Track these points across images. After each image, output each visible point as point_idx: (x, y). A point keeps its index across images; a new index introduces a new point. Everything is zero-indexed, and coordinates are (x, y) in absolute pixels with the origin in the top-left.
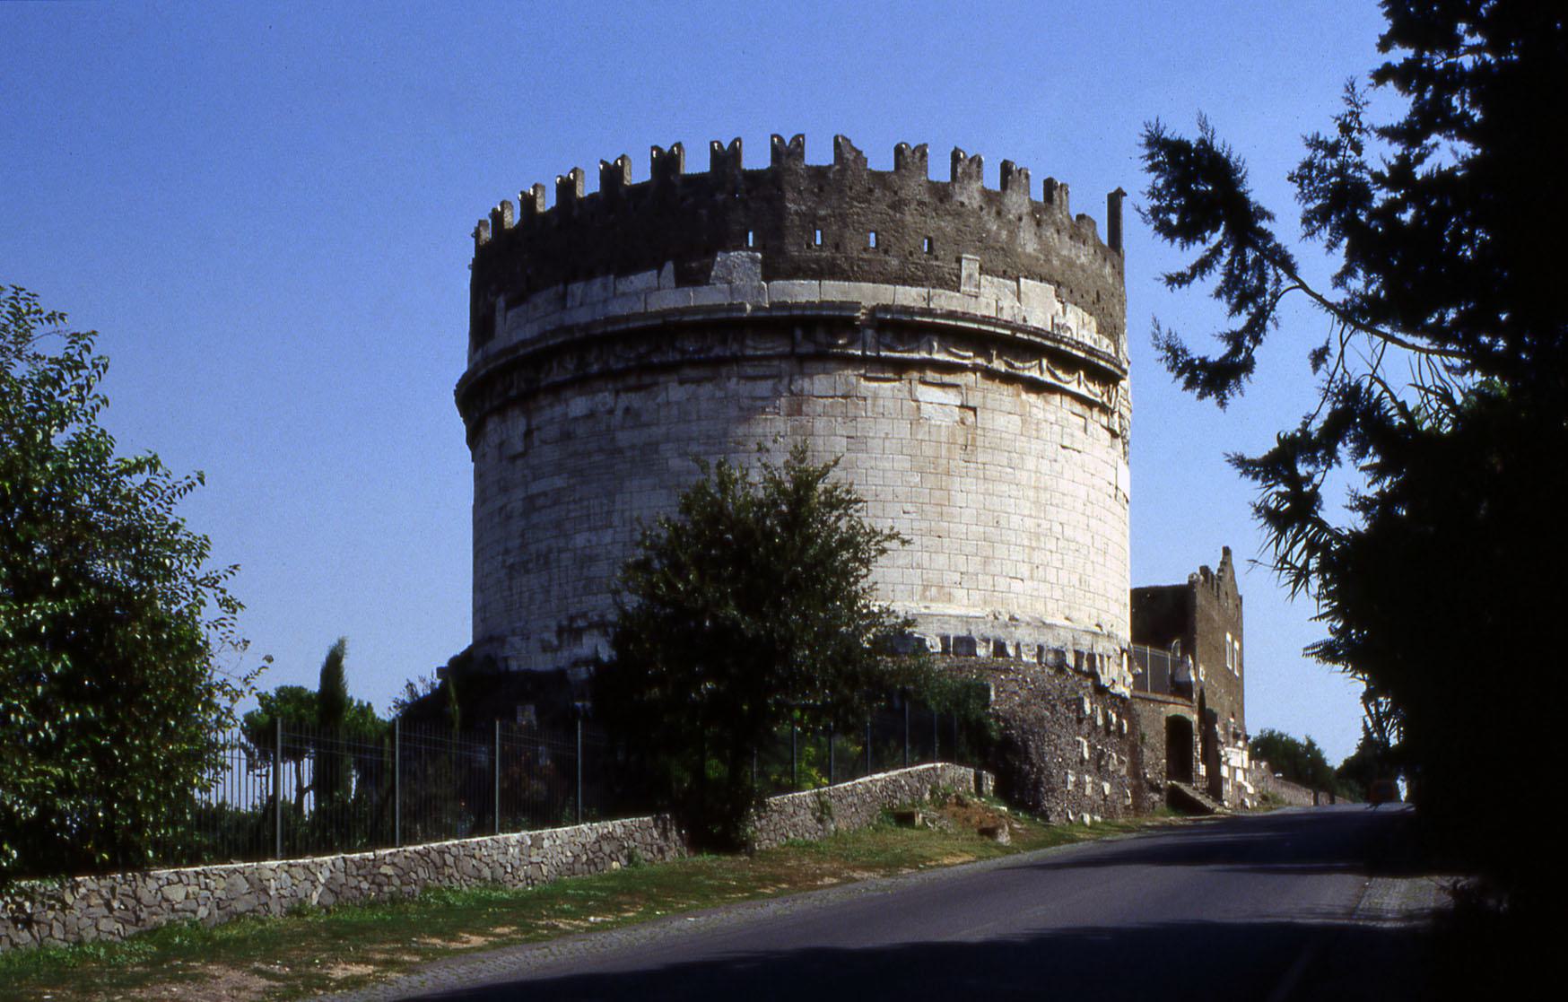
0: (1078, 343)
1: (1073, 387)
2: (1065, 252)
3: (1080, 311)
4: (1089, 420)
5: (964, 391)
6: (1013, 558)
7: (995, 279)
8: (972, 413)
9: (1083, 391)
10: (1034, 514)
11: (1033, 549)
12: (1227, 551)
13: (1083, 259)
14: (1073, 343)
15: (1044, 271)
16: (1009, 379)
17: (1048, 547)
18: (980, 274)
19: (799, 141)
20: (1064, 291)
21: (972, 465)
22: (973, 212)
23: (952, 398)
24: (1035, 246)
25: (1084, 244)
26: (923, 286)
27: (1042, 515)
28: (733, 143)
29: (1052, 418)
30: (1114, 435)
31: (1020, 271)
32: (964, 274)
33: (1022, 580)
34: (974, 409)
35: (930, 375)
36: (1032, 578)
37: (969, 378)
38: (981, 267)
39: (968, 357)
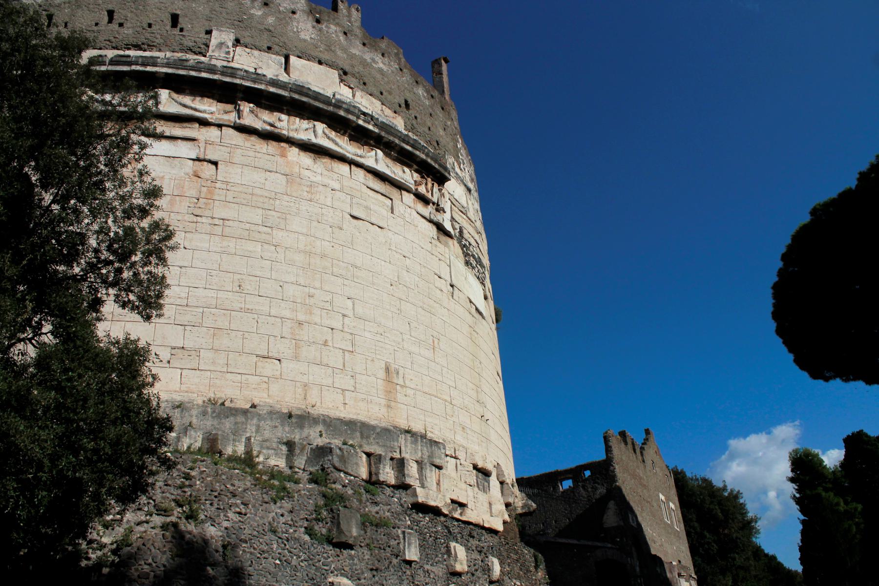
0: (365, 114)
1: (370, 162)
2: (354, 51)
3: (378, 103)
4: (397, 202)
5: (202, 145)
6: (261, 331)
7: (256, 53)
8: (214, 167)
12: (647, 432)
13: (381, 65)
14: (357, 111)
15: (325, 57)
17: (327, 322)
18: (234, 46)
20: (353, 82)
21: (204, 220)
23: (185, 150)
24: (313, 36)
25: (383, 55)
26: (160, 50)
27: (318, 285)
29: (336, 186)
30: (440, 228)
32: (214, 42)
33: (279, 360)
34: (215, 164)
36: (296, 358)
37: (214, 132)
39: (208, 108)
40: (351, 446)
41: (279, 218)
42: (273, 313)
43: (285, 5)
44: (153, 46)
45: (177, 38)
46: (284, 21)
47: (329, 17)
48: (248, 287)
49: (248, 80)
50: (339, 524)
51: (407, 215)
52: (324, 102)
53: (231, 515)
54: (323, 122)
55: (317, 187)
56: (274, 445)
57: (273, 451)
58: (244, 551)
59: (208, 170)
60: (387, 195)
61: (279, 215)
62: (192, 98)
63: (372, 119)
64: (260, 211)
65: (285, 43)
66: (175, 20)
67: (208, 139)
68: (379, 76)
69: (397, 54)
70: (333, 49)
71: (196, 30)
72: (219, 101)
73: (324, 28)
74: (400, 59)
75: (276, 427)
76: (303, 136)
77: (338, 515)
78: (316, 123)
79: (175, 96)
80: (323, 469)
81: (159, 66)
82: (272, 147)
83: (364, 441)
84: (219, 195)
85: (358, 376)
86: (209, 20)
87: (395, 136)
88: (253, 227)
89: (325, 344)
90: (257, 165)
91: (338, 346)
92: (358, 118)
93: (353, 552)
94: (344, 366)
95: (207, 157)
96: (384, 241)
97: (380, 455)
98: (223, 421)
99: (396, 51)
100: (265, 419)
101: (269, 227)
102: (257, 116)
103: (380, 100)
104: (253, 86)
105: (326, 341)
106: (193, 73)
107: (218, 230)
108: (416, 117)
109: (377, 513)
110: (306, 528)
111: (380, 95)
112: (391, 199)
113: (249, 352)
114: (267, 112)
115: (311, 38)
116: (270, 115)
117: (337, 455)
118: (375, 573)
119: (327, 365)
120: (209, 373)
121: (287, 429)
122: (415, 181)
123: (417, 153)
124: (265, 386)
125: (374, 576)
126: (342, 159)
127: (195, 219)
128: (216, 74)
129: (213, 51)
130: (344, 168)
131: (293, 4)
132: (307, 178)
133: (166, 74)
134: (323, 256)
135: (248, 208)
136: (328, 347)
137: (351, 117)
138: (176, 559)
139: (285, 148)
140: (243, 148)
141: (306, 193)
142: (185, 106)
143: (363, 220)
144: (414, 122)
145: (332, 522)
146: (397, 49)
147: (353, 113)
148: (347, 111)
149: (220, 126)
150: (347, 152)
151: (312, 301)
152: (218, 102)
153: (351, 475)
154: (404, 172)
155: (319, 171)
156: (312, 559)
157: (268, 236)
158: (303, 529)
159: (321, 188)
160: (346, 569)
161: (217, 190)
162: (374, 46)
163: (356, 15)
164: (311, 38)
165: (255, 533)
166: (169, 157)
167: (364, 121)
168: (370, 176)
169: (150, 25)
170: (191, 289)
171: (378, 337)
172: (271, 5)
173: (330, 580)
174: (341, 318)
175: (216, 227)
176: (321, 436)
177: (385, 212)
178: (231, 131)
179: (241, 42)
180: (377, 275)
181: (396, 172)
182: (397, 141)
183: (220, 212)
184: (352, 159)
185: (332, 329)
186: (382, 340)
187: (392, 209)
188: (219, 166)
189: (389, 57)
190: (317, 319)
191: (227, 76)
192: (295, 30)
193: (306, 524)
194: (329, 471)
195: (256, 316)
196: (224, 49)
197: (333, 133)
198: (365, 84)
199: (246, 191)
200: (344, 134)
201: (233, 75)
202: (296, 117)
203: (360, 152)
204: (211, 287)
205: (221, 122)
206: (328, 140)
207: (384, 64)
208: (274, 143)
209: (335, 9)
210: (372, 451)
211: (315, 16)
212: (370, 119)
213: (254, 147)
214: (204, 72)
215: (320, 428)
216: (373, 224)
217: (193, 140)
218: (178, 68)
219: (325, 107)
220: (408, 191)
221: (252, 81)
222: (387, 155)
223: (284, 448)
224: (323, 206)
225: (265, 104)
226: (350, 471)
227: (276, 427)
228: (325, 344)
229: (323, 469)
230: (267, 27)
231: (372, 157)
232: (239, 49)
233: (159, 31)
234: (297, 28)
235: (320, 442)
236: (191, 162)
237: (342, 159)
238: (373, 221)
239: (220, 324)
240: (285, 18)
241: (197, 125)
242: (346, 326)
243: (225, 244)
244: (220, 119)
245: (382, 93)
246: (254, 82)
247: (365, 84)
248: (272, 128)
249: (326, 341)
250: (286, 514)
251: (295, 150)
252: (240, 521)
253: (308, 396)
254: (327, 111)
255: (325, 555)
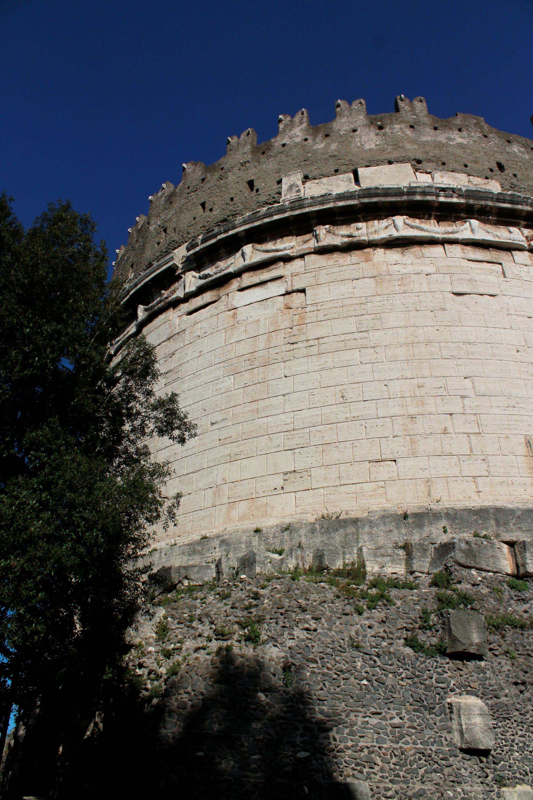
0: (443, 190)
6: (372, 435)
8: (303, 294)
10: (408, 374)
11: (413, 417)
13: (459, 140)
14: (434, 190)
18: (304, 183)
21: (300, 345)
22: (296, 145)
24: (377, 143)
25: (460, 130)
29: (430, 269)
31: (357, 164)
33: (395, 461)
34: (303, 291)
35: (247, 279)
36: (414, 454)
37: (298, 264)
40: (485, 537)
41: (373, 319)
42: (381, 414)
43: (345, 128)
44: (237, 214)
45: (254, 199)
46: (346, 142)
47: (391, 120)
48: (351, 395)
49: (316, 205)
50: (450, 629)
51: (523, 274)
52: (396, 195)
53: (297, 632)
54: (402, 215)
55: (409, 277)
56: (390, 551)
57: (389, 558)
58: (313, 673)
59: (298, 298)
60: (494, 261)
61: (373, 316)
62: (273, 242)
63: (454, 192)
64: (353, 320)
65: (351, 160)
66: (251, 184)
67: (293, 272)
68: (459, 151)
69: (477, 124)
70: (401, 145)
71: (269, 185)
72: (298, 235)
73: (388, 131)
74: (482, 128)
75: (390, 531)
76: (384, 235)
77: (448, 618)
78: (394, 218)
79: (258, 246)
80: (447, 568)
81: (238, 227)
82: (355, 256)
83: (502, 528)
84: (310, 317)
85: (490, 458)
86: (278, 171)
87: (486, 199)
88: (348, 337)
89: (445, 431)
90: (342, 278)
91: (460, 431)
92: (438, 196)
93: (483, 663)
94: (471, 451)
95: (294, 288)
96: (499, 308)
97: (524, 542)
98: (333, 535)
99: (475, 121)
100: (377, 525)
101: (365, 331)
102: (334, 234)
103: (465, 173)
104: (321, 208)
105: (445, 429)
106: (267, 220)
107: (314, 350)
108: (515, 175)
109: (526, 612)
110: (405, 639)
111: (465, 169)
112: (500, 264)
113: (360, 460)
114: (344, 227)
115: (376, 145)
116: (348, 228)
117: (462, 550)
118: (522, 688)
119: (451, 455)
120: (322, 490)
121: (403, 531)
122: (527, 237)
123: (520, 207)
124: (382, 491)
125: (521, 692)
126: (432, 242)
127: (292, 347)
128: (285, 212)
129: (285, 196)
130: (438, 250)
131: (352, 124)
132: (398, 273)
133: (246, 231)
134: (428, 342)
135: (340, 321)
136: (448, 435)
137: (429, 198)
138: (215, 686)
139: (369, 253)
140: (327, 267)
141: (398, 287)
142: (267, 251)
143: (469, 294)
144: (514, 181)
145: (443, 629)
146: (476, 119)
147: (430, 194)
148: (424, 193)
149: (302, 256)
150: (436, 233)
151: (423, 391)
152: (297, 236)
153: (489, 571)
154: (510, 232)
155: (409, 261)
156: (418, 676)
157: (364, 340)
158: (402, 641)
159: (414, 276)
160: (475, 685)
161: (308, 314)
162: (446, 126)
163: (420, 106)
164: (376, 145)
165: (329, 650)
166: (262, 301)
167: (446, 196)
168: (468, 248)
169: (232, 199)
170: (296, 413)
171: (510, 411)
172: (332, 134)
173: (449, 700)
174: (460, 401)
175: (312, 348)
176: (445, 531)
178: (313, 256)
179: (310, 177)
180: (497, 345)
181: (499, 234)
182: (490, 203)
183: (313, 332)
184: (443, 239)
185: (451, 414)
186: (517, 413)
187: (504, 273)
188: (307, 291)
189: (467, 129)
190: (432, 409)
191: (296, 209)
192: (359, 144)
193: (405, 634)
194: (452, 569)
195: (363, 422)
196: (295, 189)
197: (417, 221)
198: (444, 164)
199: (336, 305)
200: (429, 218)
201: (301, 207)
202: (374, 220)
203: (450, 229)
204: (313, 406)
205: (302, 253)
206: (411, 229)
207: (464, 138)
208: (357, 252)
209: (397, 109)
210: (514, 539)
211: (376, 125)
212: (451, 193)
213: (337, 263)
214: (276, 215)
215: (444, 523)
216: (482, 295)
217: (280, 277)
218: (253, 222)
219: (398, 199)
220: (520, 249)
221: (320, 204)
222: (485, 222)
223: (401, 552)
224: (419, 294)
225: (340, 220)
226: (484, 566)
227: (390, 531)
228: (445, 431)
229: (447, 568)
230: (331, 154)
231: (466, 229)
232: (308, 184)
233: (239, 200)
234: (360, 142)
235: (444, 539)
236: (282, 297)
237: (432, 242)
238: (481, 292)
239: (327, 440)
240: (347, 139)
241: (282, 263)
242: (467, 408)
243: (322, 360)
244: (300, 250)
245: (466, 166)
246: (322, 204)
247: (444, 164)
248: (350, 239)
249: (445, 429)
250: (376, 624)
251: (380, 251)
252: (308, 638)
253: (432, 491)
254: (403, 202)
255: (439, 670)
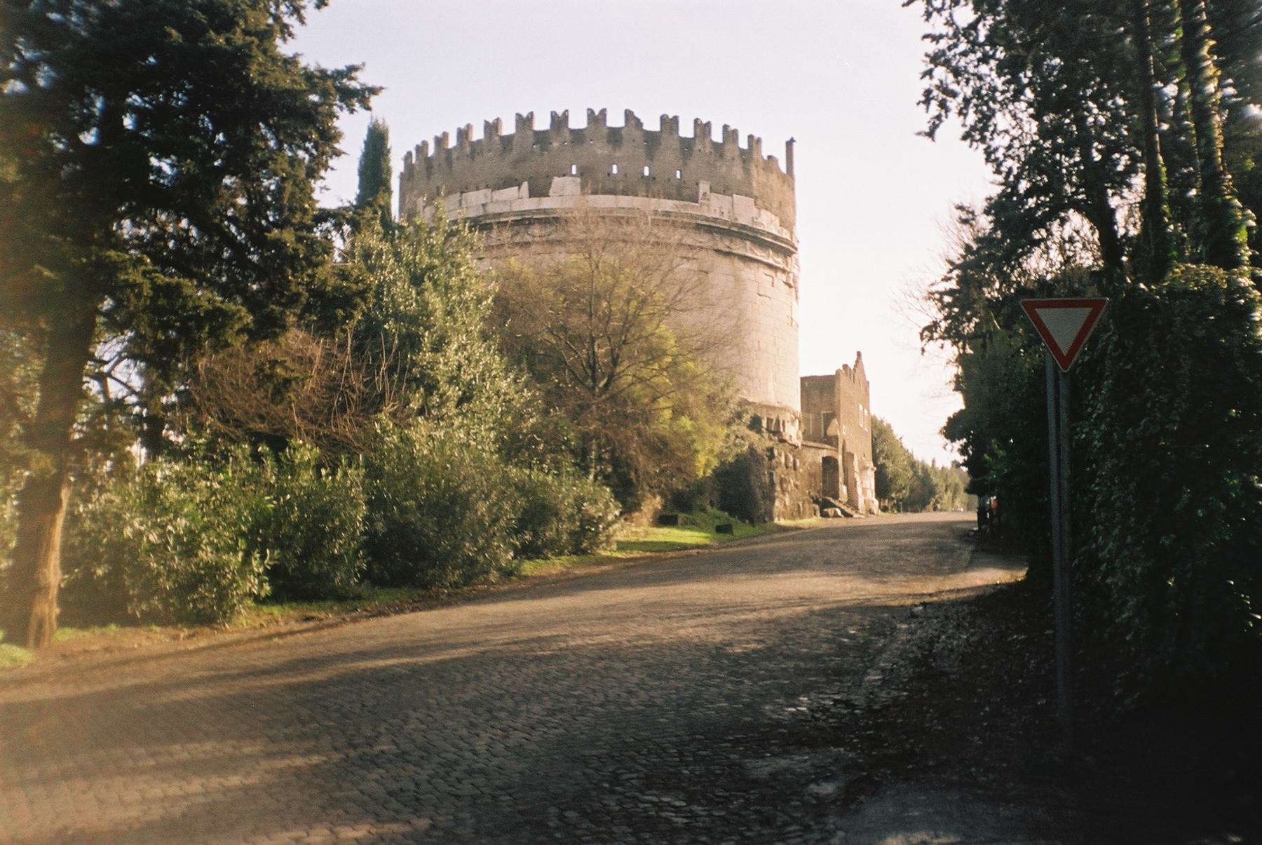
9: (770, 261)
12: (859, 354)
16: (729, 254)
19: (603, 112)
28: (564, 114)
37: (702, 254)
38: (711, 188)
39: (704, 239)
177: (769, 286)
